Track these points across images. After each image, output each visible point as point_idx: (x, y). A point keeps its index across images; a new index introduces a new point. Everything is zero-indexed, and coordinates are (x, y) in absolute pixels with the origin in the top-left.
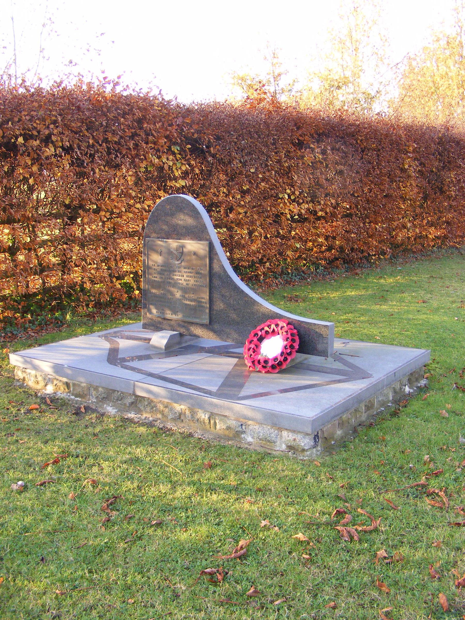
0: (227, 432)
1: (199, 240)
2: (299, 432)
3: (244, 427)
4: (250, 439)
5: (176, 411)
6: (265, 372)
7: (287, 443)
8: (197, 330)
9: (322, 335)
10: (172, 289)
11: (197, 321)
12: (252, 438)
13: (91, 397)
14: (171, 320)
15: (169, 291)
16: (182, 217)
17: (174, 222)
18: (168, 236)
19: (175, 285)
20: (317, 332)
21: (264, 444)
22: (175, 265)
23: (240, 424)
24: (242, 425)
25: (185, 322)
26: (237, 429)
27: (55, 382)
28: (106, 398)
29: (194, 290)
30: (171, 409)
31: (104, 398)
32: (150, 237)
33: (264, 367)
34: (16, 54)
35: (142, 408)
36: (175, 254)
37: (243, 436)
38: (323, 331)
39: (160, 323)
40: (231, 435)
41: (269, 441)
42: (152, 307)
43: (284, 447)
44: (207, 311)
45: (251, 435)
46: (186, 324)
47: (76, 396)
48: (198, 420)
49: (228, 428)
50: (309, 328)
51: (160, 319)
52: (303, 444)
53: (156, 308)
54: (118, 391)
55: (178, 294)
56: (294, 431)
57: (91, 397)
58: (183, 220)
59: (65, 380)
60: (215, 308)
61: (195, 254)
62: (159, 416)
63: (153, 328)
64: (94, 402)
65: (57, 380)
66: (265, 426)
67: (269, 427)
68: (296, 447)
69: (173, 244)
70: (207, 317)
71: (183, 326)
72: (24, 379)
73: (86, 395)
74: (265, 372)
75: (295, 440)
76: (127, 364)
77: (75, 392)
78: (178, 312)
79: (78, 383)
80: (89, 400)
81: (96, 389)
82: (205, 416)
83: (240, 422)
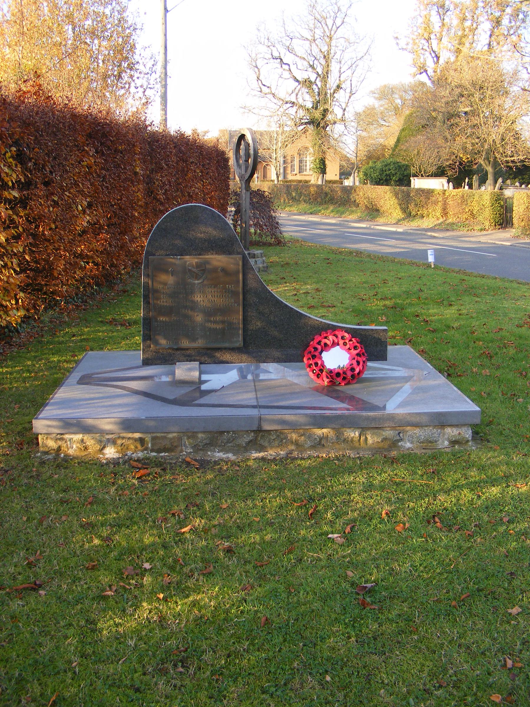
0: (381, 445)
1: (227, 254)
2: (464, 425)
3: (401, 435)
4: (408, 445)
5: (316, 437)
6: (345, 384)
7: (450, 438)
8: (225, 356)
9: (380, 339)
10: (190, 313)
11: (227, 345)
12: (411, 443)
13: (184, 448)
14: (187, 349)
15: (186, 316)
16: (203, 229)
17: (191, 236)
18: (183, 252)
19: (194, 307)
20: (374, 337)
21: (425, 446)
22: (195, 284)
23: (397, 432)
24: (399, 433)
25: (208, 349)
26: (395, 439)
27: (119, 442)
28: (209, 444)
29: (224, 311)
30: (310, 437)
31: (206, 444)
32: (154, 255)
33: (344, 379)
34: (405, 51)
35: (266, 444)
36: (194, 272)
37: (400, 444)
38: (382, 335)
39: (170, 355)
40: (386, 447)
41: (430, 442)
42: (158, 337)
43: (446, 443)
44: (241, 332)
45: (409, 441)
46: (209, 352)
47: (159, 451)
48: (345, 439)
49: (385, 439)
50: (365, 335)
51: (170, 351)
52: (468, 436)
53: (165, 338)
54: (228, 432)
55: (199, 318)
56: (456, 426)
57: (184, 448)
58: (204, 232)
59: (137, 435)
60: (251, 327)
61: (224, 270)
62: (293, 447)
63: (159, 362)
64: (191, 452)
65: (123, 438)
66: (426, 428)
67: (431, 428)
68: (460, 441)
69: (191, 260)
70: (241, 338)
71: (206, 354)
72: (59, 448)
73: (176, 447)
74: (345, 384)
75: (460, 434)
76: (196, 402)
77: (156, 448)
78: (197, 338)
79: (163, 435)
80: (182, 451)
81: (193, 435)
82: (355, 434)
83: (397, 430)
